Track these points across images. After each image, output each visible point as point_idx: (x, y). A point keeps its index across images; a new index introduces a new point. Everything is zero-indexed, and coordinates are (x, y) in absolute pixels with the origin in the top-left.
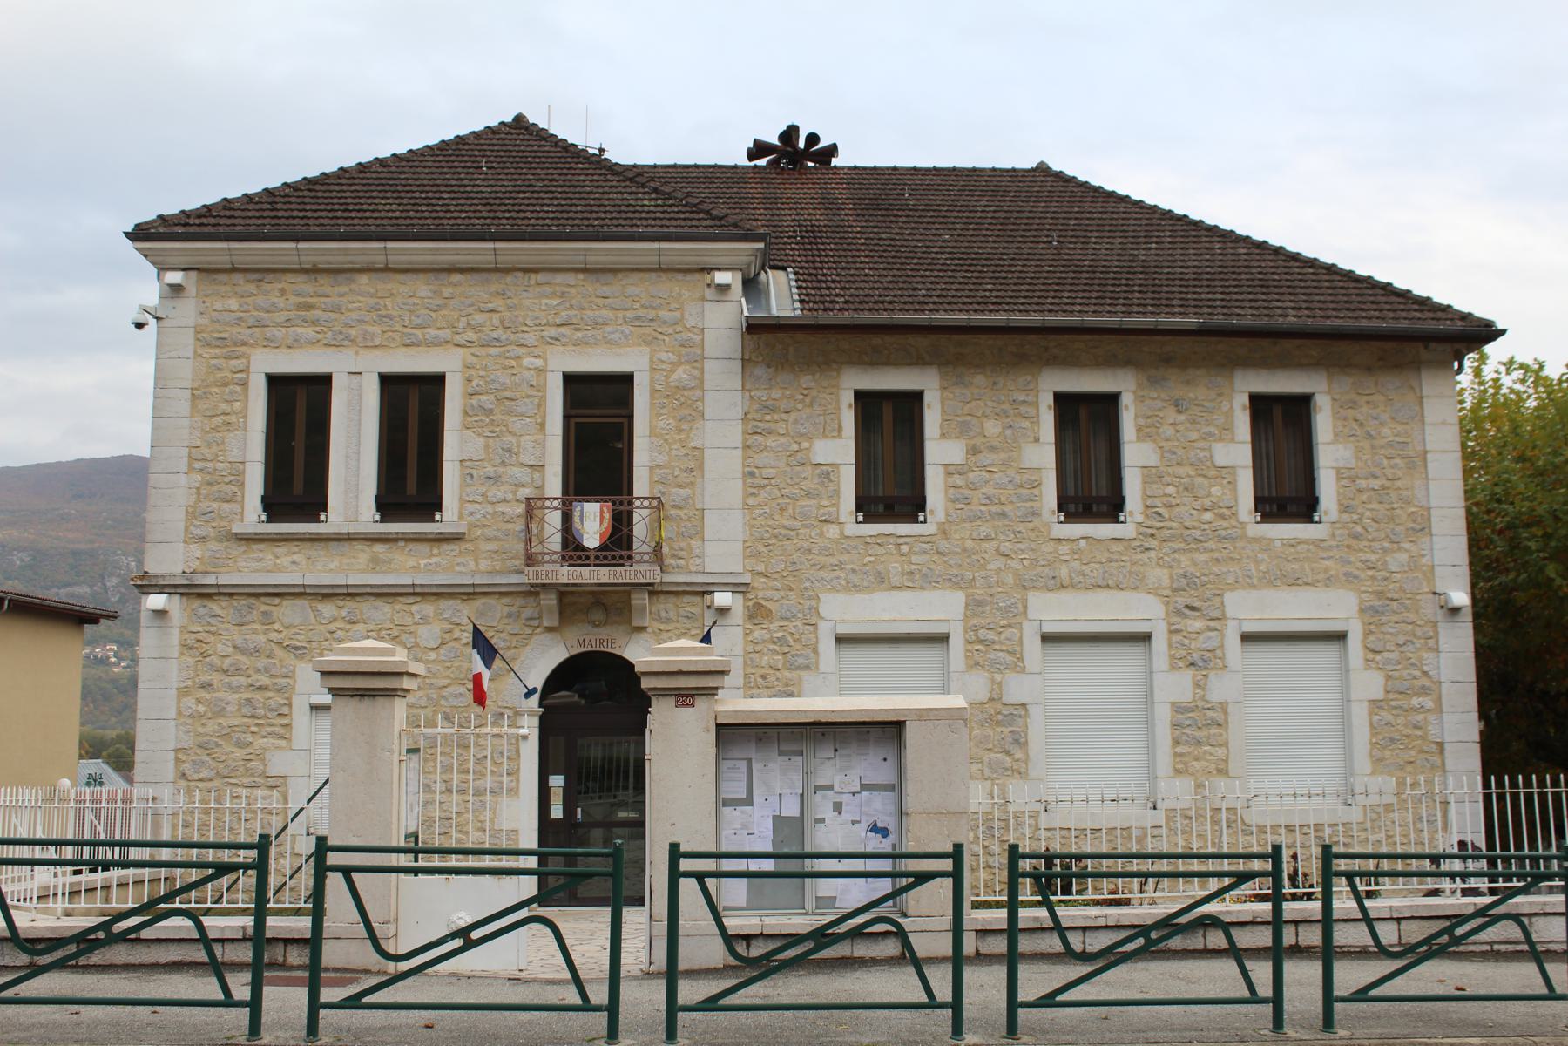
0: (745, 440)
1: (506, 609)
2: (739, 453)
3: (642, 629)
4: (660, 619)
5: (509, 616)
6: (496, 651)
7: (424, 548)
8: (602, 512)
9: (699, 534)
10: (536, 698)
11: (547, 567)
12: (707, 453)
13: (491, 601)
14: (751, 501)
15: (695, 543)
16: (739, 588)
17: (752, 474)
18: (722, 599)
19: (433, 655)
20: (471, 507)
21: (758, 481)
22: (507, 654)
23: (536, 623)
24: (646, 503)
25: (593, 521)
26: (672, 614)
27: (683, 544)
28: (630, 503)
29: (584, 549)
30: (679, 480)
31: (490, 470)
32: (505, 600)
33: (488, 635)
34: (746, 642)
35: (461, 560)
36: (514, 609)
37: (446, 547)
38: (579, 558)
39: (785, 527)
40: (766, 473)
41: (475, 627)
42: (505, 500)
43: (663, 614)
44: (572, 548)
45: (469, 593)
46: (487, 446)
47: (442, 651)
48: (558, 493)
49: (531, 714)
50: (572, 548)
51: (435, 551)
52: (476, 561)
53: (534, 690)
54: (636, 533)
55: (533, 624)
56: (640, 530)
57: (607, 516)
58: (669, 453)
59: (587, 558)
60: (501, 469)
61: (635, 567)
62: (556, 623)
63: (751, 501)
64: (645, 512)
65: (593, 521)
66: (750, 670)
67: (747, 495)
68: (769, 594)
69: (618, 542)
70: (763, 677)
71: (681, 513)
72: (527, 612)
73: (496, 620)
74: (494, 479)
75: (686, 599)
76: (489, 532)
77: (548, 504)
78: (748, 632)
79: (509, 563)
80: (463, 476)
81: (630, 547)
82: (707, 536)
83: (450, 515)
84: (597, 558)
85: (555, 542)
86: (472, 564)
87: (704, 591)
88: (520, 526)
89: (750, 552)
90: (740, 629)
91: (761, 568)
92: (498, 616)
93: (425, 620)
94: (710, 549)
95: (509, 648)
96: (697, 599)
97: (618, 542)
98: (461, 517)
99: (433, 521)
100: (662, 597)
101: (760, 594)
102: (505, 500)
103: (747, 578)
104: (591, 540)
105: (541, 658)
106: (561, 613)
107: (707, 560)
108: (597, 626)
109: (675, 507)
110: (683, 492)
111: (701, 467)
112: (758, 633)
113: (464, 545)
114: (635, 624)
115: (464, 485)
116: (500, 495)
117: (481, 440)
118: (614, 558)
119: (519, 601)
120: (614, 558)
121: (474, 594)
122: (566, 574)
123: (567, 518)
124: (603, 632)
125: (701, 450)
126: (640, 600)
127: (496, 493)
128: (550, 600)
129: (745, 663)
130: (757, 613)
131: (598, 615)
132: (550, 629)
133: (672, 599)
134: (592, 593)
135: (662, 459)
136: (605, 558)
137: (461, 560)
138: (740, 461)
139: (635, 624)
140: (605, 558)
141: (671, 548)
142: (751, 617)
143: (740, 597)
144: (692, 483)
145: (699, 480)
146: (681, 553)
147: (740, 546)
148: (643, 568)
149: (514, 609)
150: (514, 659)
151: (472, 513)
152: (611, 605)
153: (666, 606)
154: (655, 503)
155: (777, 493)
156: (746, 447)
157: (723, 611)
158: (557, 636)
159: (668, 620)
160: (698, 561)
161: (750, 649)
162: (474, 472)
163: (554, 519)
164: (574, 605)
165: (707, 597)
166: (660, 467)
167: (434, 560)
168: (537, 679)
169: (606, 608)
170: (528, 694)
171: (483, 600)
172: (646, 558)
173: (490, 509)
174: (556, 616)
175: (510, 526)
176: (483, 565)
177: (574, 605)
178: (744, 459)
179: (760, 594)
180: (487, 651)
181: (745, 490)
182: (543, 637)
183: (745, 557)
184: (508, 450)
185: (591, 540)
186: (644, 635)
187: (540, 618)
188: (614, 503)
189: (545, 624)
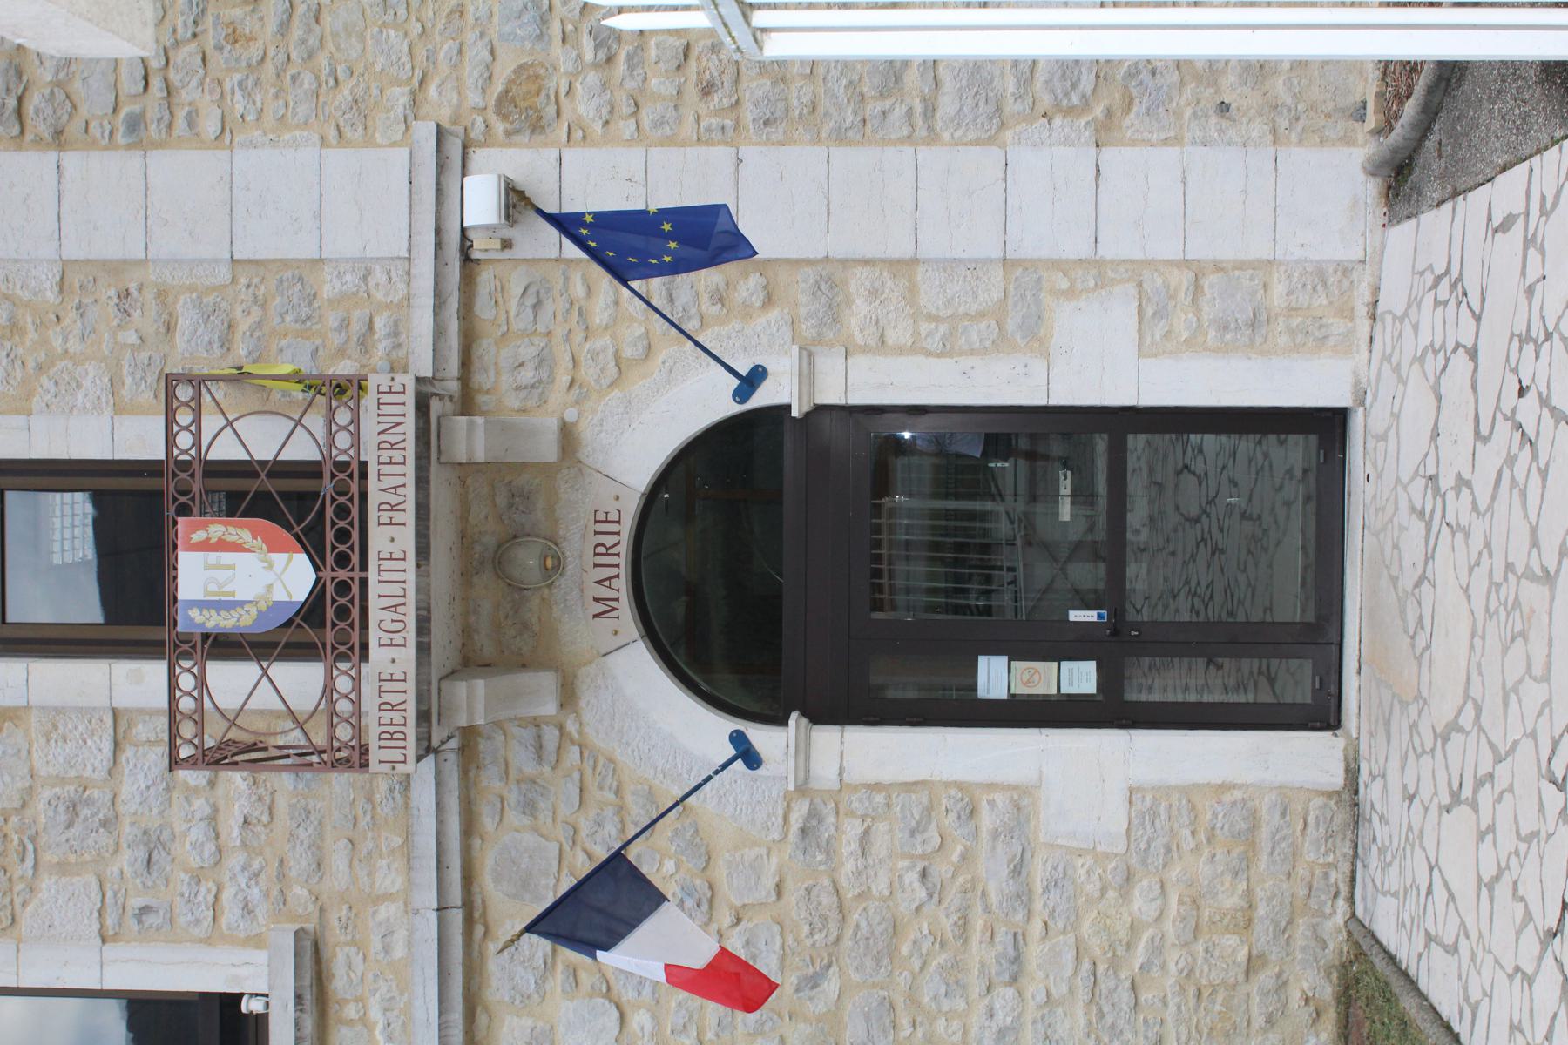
0: (39, 143)
1: (513, 817)
2: (71, 159)
3: (568, 436)
5: (530, 808)
8: (205, 546)
9: (300, 273)
10: (761, 736)
11: (369, 701)
12: (72, 251)
13: (488, 861)
16: (452, 155)
17: (135, 124)
18: (480, 203)
20: (231, 914)
22: (639, 815)
23: (551, 736)
24: (184, 418)
25: (235, 573)
26: (528, 352)
27: (332, 320)
28: (185, 466)
29: (317, 595)
31: (127, 861)
32: (488, 822)
33: (584, 867)
35: (376, 944)
36: (513, 797)
37: (339, 984)
38: (342, 613)
39: (284, 27)
41: (530, 928)
42: (212, 819)
43: (527, 375)
44: (322, 627)
45: (465, 912)
46: (62, 868)
48: (153, 673)
49: (803, 750)
50: (322, 627)
51: (351, 1011)
52: (387, 897)
53: (738, 739)
56: (260, 438)
57: (217, 529)
59: (343, 588)
60: (127, 831)
61: (369, 455)
62: (547, 681)
63: (210, 126)
65: (235, 573)
67: (195, 138)
68: (472, 74)
69: (304, 504)
70: (707, 91)
71: (244, 325)
72: (522, 760)
73: (537, 860)
74: (153, 850)
75: (484, 309)
76: (299, 864)
77: (186, 704)
78: (578, 135)
79: (385, 810)
81: (310, 470)
82: (308, 251)
83: (255, 973)
84: (343, 560)
85: (300, 681)
86: (386, 911)
88: (283, 782)
89: (352, 126)
90: (568, 155)
91: (399, 97)
92: (529, 839)
94: (343, 243)
95: (620, 809)
97: (304, 504)
98: (256, 941)
99: (261, 1020)
100: (480, 379)
101: (474, 98)
102: (212, 819)
103: (425, 133)
104: (291, 577)
105: (656, 719)
107: (369, 253)
109: (226, 343)
110: (186, 320)
111: (115, 268)
112: (584, 107)
113: (335, 935)
116: (197, 833)
117: (47, 883)
118: (343, 512)
119: (489, 780)
120: (343, 512)
121: (468, 905)
122: (391, 655)
123: (225, 646)
124: (577, 546)
125: (66, 266)
126: (470, 440)
127: (191, 845)
128: (473, 700)
129: (670, 141)
130: (525, 108)
131: (527, 560)
132: (568, 696)
133: (486, 349)
134: (466, 575)
135: (93, 378)
136: (342, 536)
137: (376, 944)
138: (95, 156)
140: (342, 536)
141: (341, 352)
142: (537, 126)
143: (478, 156)
144: (161, 294)
146: (357, 327)
147: (337, 158)
148: (370, 426)
149: (513, 797)
150: (651, 795)
151: (247, 909)
153: (502, 372)
154: (184, 393)
155: (186, 54)
156: (59, 138)
157: (516, 200)
159: (544, 360)
160: (379, 276)
161: (627, 128)
162: (135, 902)
163: (231, 681)
165: (481, 246)
166: (114, 385)
167: (375, 1014)
168: (704, 731)
169: (515, 537)
170: (747, 755)
172: (343, 417)
173: (235, 861)
174: (526, 679)
175: (282, 805)
176: (389, 878)
177: (494, 624)
178: (93, 145)
179: (474, 98)
180: (601, 906)
182: (588, 716)
183: (369, 142)
184: (73, 808)
185: (291, 577)
187: (536, 722)
188: (184, 510)
189: (549, 708)
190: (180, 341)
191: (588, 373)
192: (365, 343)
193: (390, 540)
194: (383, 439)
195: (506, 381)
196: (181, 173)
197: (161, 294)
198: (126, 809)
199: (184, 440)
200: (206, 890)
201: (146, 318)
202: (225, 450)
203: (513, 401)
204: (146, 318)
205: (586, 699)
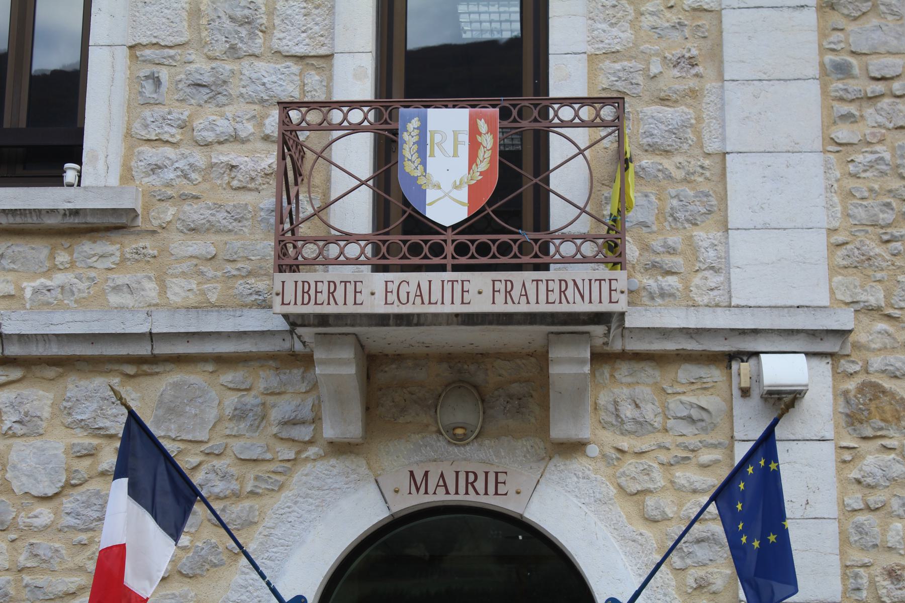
1: (232, 400)
4: (619, 424)
5: (240, 414)
6: (197, 493)
7: (35, 251)
8: (474, 131)
11: (337, 273)
12: (729, 18)
13: (194, 377)
14: (843, 133)
15: (703, 236)
17: (843, 70)
18: (782, 369)
19: (44, 514)
21: (859, 85)
22: (232, 513)
23: (305, 433)
24: (586, 113)
26: (649, 411)
27: (674, 239)
28: (544, 114)
29: (433, 228)
30: (662, 84)
31: (201, 68)
32: (228, 377)
33: (185, 462)
34: (844, 483)
35: (121, 279)
36: (250, 399)
37: (87, 247)
38: (415, 250)
40: (877, 65)
41: (132, 414)
42: (235, 138)
43: (628, 411)
44: (403, 232)
45: (147, 357)
47: (67, 503)
48: (365, 90)
50: (403, 232)
51: (62, 258)
52: (163, 288)
54: (556, 181)
55: (300, 436)
56: (569, 176)
57: (488, 141)
58: (634, 24)
59: (437, 250)
60: (228, 66)
62: (354, 430)
63: (843, 133)
64: (582, 136)
66: (857, 557)
71: (668, 164)
72: (284, 407)
73: (193, 418)
74: (210, 90)
75: (686, 372)
76: (194, 213)
77: (336, 116)
78: (847, 457)
79: (240, 286)
80: (135, 81)
82: (735, 217)
83: (100, 174)
84: (462, 249)
85: (356, 213)
86: (151, 290)
87: (730, 353)
88: (267, 200)
90: (828, 449)
91: (875, 297)
92: (212, 415)
93: (29, 426)
94: (743, 249)
95: (237, 496)
96: (714, 374)
98: (127, 176)
99: (57, 180)
100: (623, 370)
101: (877, 362)
102: (235, 138)
103: (844, 320)
104: (447, 207)
106: (368, 409)
107: (735, 274)
108: (458, 440)
109: (652, 149)
110: (672, 114)
111: (716, 54)
112: (872, 462)
113: (131, 244)
114: (560, 430)
115: (138, 103)
116: (224, 126)
118: (504, 249)
119: (265, 379)
120: (504, 249)
121: (154, 360)
122: (379, 292)
123: (387, 150)
124: (475, 457)
125: (716, 14)
126: (568, 364)
127: (213, 121)
128: (339, 366)
129: (844, 540)
131: (461, 413)
132: (340, 449)
133: (650, 373)
134: (449, 358)
135: (620, 36)
136: (483, 249)
137: (121, 279)
138: (814, 37)
139: (560, 430)
140: (483, 249)
141: (645, 248)
142: (853, 418)
143: (824, 367)
144: (694, 94)
145: (710, 85)
146: (668, 261)
147: (818, 243)
149: (250, 399)
150: (250, 524)
151: (156, 168)
152: (495, 385)
153: (631, 392)
154: (608, 113)
157: (784, 401)
158: (359, 465)
159: (642, 426)
160: (714, 280)
161: (855, 500)
162: (164, 74)
163: (356, 154)
164: (406, 383)
165: (745, 368)
166: (613, 55)
167: (59, 278)
169: (482, 398)
171: (175, 376)
172: (588, 249)
173: (199, 158)
174: (356, 411)
175: (247, 198)
176: (180, 290)
177: (406, 383)
178: (823, 35)
179: (877, 362)
181: (827, 108)
182: (321, 467)
183: (834, 270)
184: (247, 22)
185: (447, 207)
186: (578, 465)
187: (316, 420)
188: (505, 114)
189: (329, 432)
190: (654, 110)
191: (630, 466)
192: (655, 268)
193: (480, 292)
194: (570, 285)
195: (623, 392)
196: (802, 108)
197: (694, 94)
198: (247, 68)
199: (566, 113)
200: (172, 133)
201: (673, 80)
202: (558, 148)
203: (604, 399)
204: (673, 80)
205: (336, 465)
